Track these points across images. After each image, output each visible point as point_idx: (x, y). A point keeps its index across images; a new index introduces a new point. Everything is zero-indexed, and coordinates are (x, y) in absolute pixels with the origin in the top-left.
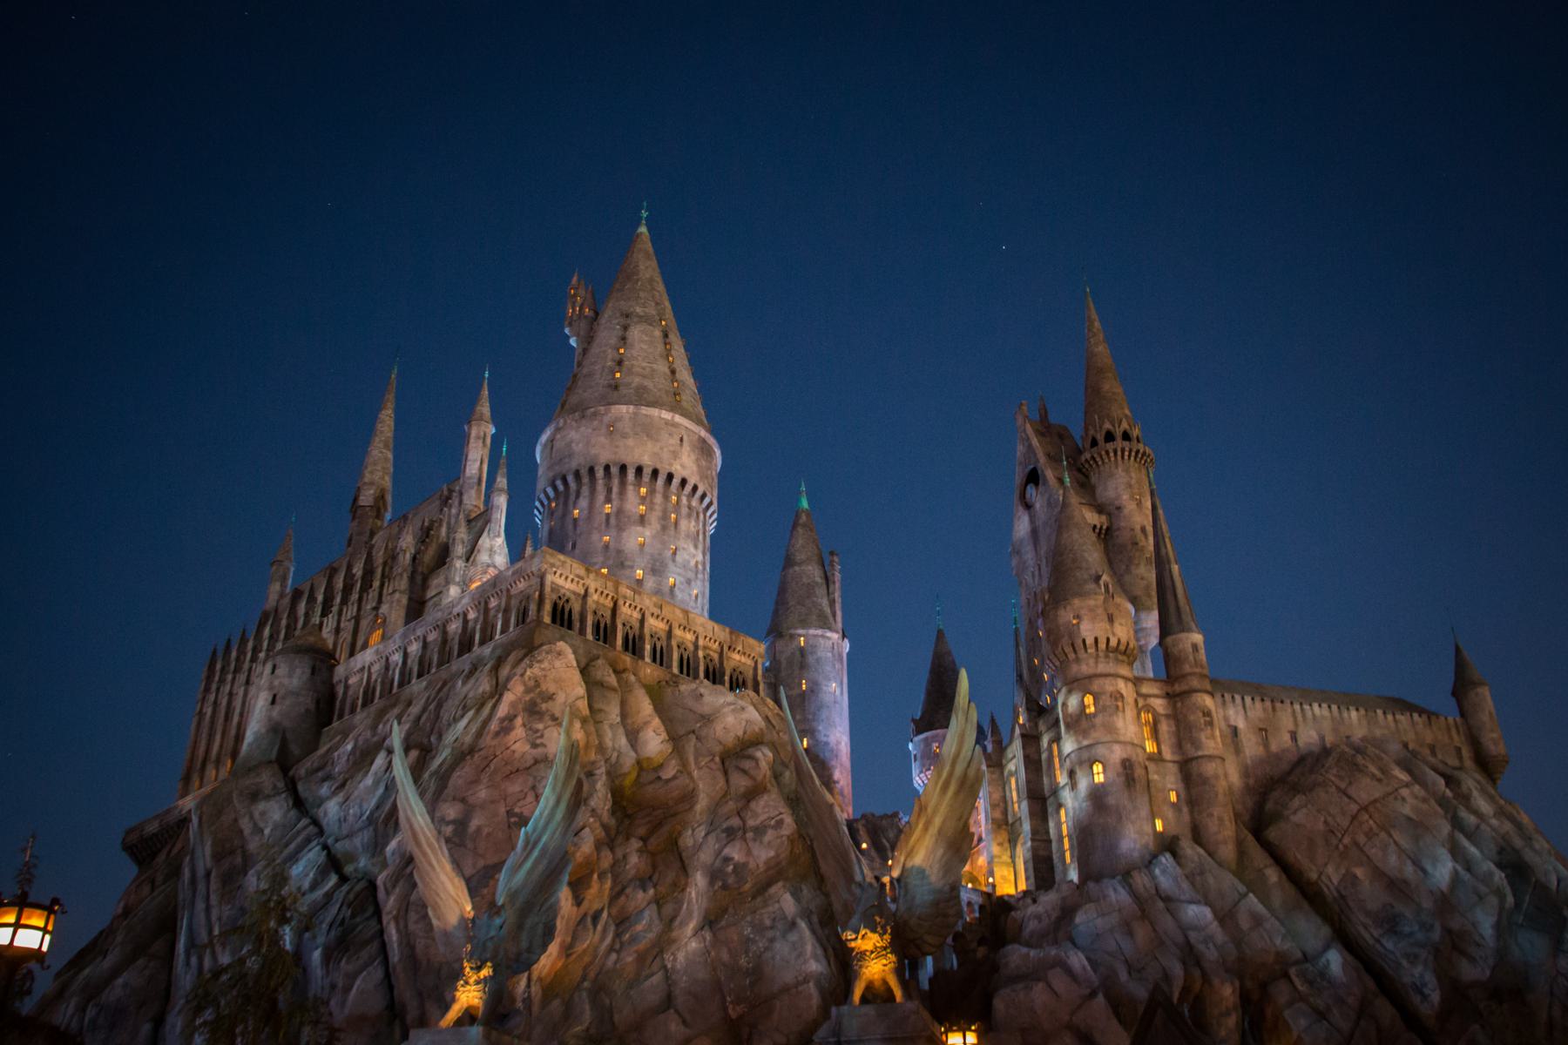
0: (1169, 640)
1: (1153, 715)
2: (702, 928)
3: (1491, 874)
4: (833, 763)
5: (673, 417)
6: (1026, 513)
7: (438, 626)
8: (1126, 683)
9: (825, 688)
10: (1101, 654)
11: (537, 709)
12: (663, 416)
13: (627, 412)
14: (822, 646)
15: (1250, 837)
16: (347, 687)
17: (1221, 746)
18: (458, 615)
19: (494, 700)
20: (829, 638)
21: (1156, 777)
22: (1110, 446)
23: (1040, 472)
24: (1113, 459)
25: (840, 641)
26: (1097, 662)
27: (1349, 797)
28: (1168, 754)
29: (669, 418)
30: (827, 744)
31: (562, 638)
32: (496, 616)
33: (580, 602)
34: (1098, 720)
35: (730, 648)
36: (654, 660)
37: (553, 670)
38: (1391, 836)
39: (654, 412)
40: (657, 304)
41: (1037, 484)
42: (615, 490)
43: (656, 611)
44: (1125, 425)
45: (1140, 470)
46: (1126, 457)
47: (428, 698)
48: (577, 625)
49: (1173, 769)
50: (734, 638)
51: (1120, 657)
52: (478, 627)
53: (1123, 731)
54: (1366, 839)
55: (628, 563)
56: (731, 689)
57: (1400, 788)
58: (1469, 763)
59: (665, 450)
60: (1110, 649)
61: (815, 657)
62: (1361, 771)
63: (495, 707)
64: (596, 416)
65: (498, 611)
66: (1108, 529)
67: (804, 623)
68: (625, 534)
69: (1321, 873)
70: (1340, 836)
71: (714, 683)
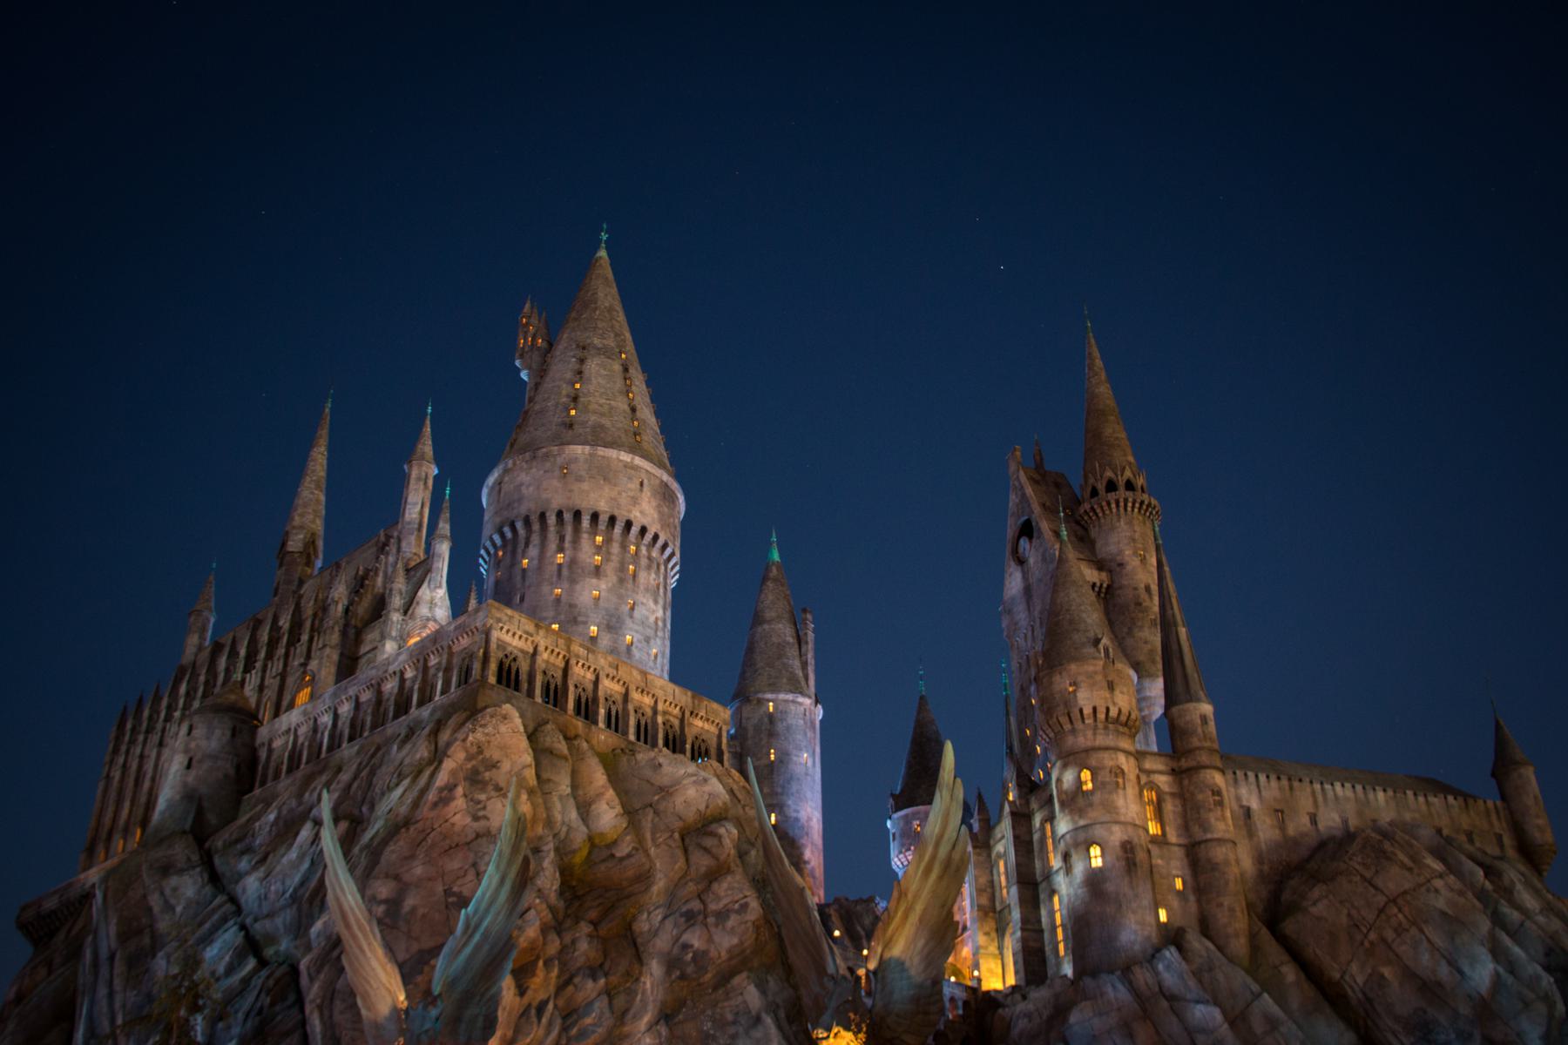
0: (1175, 710)
1: (1156, 793)
2: (657, 1023)
3: (1538, 978)
4: (803, 841)
5: (633, 459)
6: (1019, 568)
7: (372, 685)
8: (1127, 758)
9: (795, 758)
10: (1100, 726)
11: (480, 778)
12: (621, 458)
13: (583, 453)
14: (793, 712)
15: (1265, 932)
16: (270, 751)
17: (1232, 828)
18: (395, 673)
19: (432, 768)
20: (801, 704)
21: (1159, 861)
22: (1112, 496)
23: (1034, 524)
24: (1114, 510)
25: (813, 708)
26: (1095, 734)
27: (1376, 888)
28: (1173, 837)
29: (629, 460)
30: (797, 820)
31: (508, 701)
32: (435, 675)
33: (528, 661)
34: (1097, 798)
35: (692, 713)
36: (609, 725)
37: (497, 736)
38: (1422, 931)
39: (612, 453)
40: (617, 335)
41: (1030, 537)
42: (568, 538)
43: (612, 672)
44: (1128, 474)
45: (1144, 523)
46: (1129, 509)
47: (360, 764)
48: (525, 686)
49: (1179, 853)
50: (696, 702)
51: (1121, 729)
52: (416, 687)
53: (1123, 811)
54: (1394, 936)
55: (580, 619)
56: (693, 758)
57: (1432, 878)
58: (1511, 853)
60: (1110, 720)
61: (784, 724)
62: (1388, 859)
63: (433, 775)
64: (548, 457)
65: (438, 670)
66: (1109, 586)
67: (774, 688)
68: (578, 587)
69: (1344, 972)
70: (1365, 931)
71: (674, 751)
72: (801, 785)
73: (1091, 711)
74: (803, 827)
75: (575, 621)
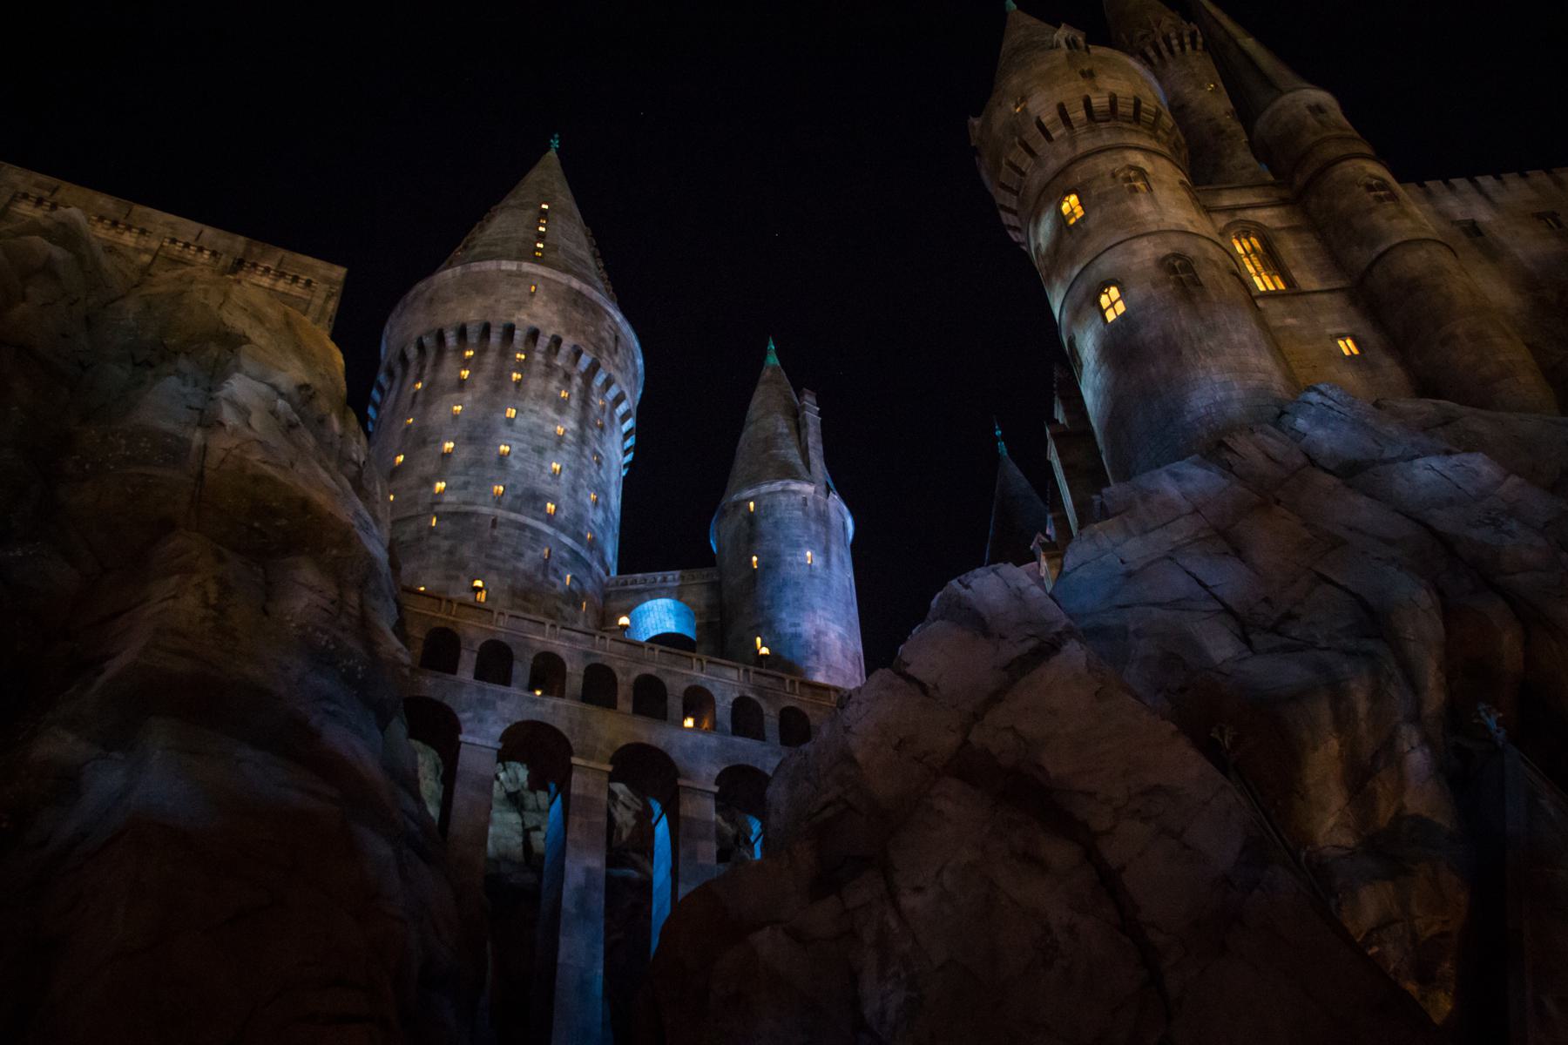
0: (1260, 125)
1: (1257, 237)
4: (811, 663)
5: (519, 266)
12: (503, 268)
14: (784, 504)
20: (795, 493)
25: (821, 497)
28: (1308, 280)
29: (515, 268)
30: (797, 636)
34: (1091, 223)
39: (490, 265)
59: (503, 301)
67: (754, 481)
68: (433, 408)
72: (802, 590)
73: (1055, 113)
74: (807, 644)
75: (424, 442)
